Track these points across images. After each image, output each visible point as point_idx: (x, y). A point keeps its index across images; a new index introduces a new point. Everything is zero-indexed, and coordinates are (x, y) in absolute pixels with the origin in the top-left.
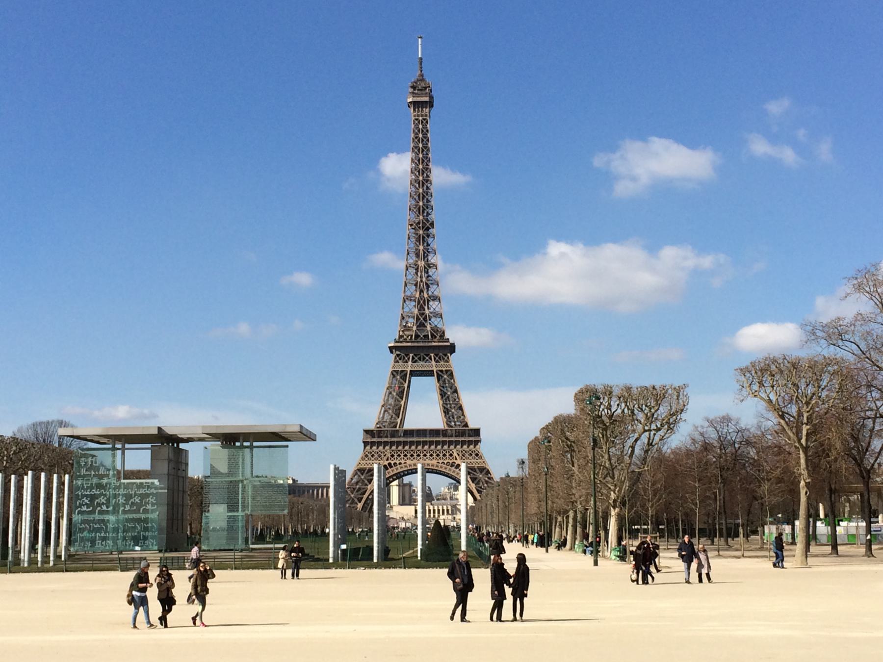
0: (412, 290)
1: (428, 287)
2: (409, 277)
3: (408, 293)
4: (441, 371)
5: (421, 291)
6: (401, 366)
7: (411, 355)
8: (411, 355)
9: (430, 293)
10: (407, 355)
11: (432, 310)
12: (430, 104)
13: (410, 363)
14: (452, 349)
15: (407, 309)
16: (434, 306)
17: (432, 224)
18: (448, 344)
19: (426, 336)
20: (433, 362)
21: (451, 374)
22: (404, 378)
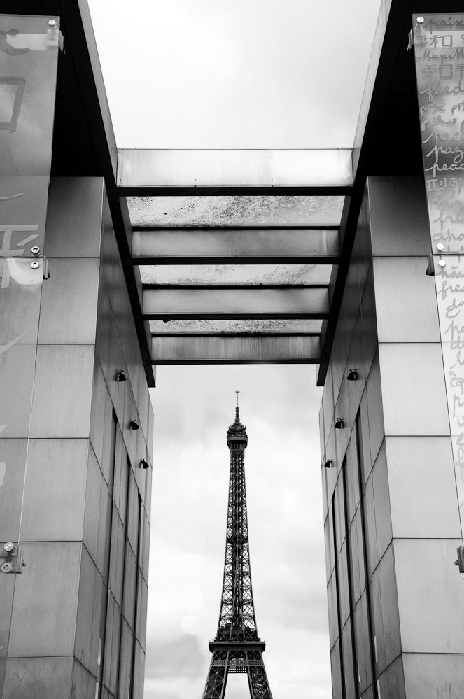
0: (228, 595)
1: (242, 593)
2: (227, 584)
3: (226, 598)
4: (254, 667)
5: (238, 596)
6: (219, 664)
7: (228, 653)
8: (228, 653)
9: (244, 598)
10: (225, 653)
11: (245, 612)
12: (244, 443)
13: (227, 660)
14: (262, 647)
15: (224, 612)
16: (247, 609)
17: (246, 540)
18: (258, 643)
19: (241, 635)
20: (247, 659)
21: (262, 671)
22: (222, 673)
